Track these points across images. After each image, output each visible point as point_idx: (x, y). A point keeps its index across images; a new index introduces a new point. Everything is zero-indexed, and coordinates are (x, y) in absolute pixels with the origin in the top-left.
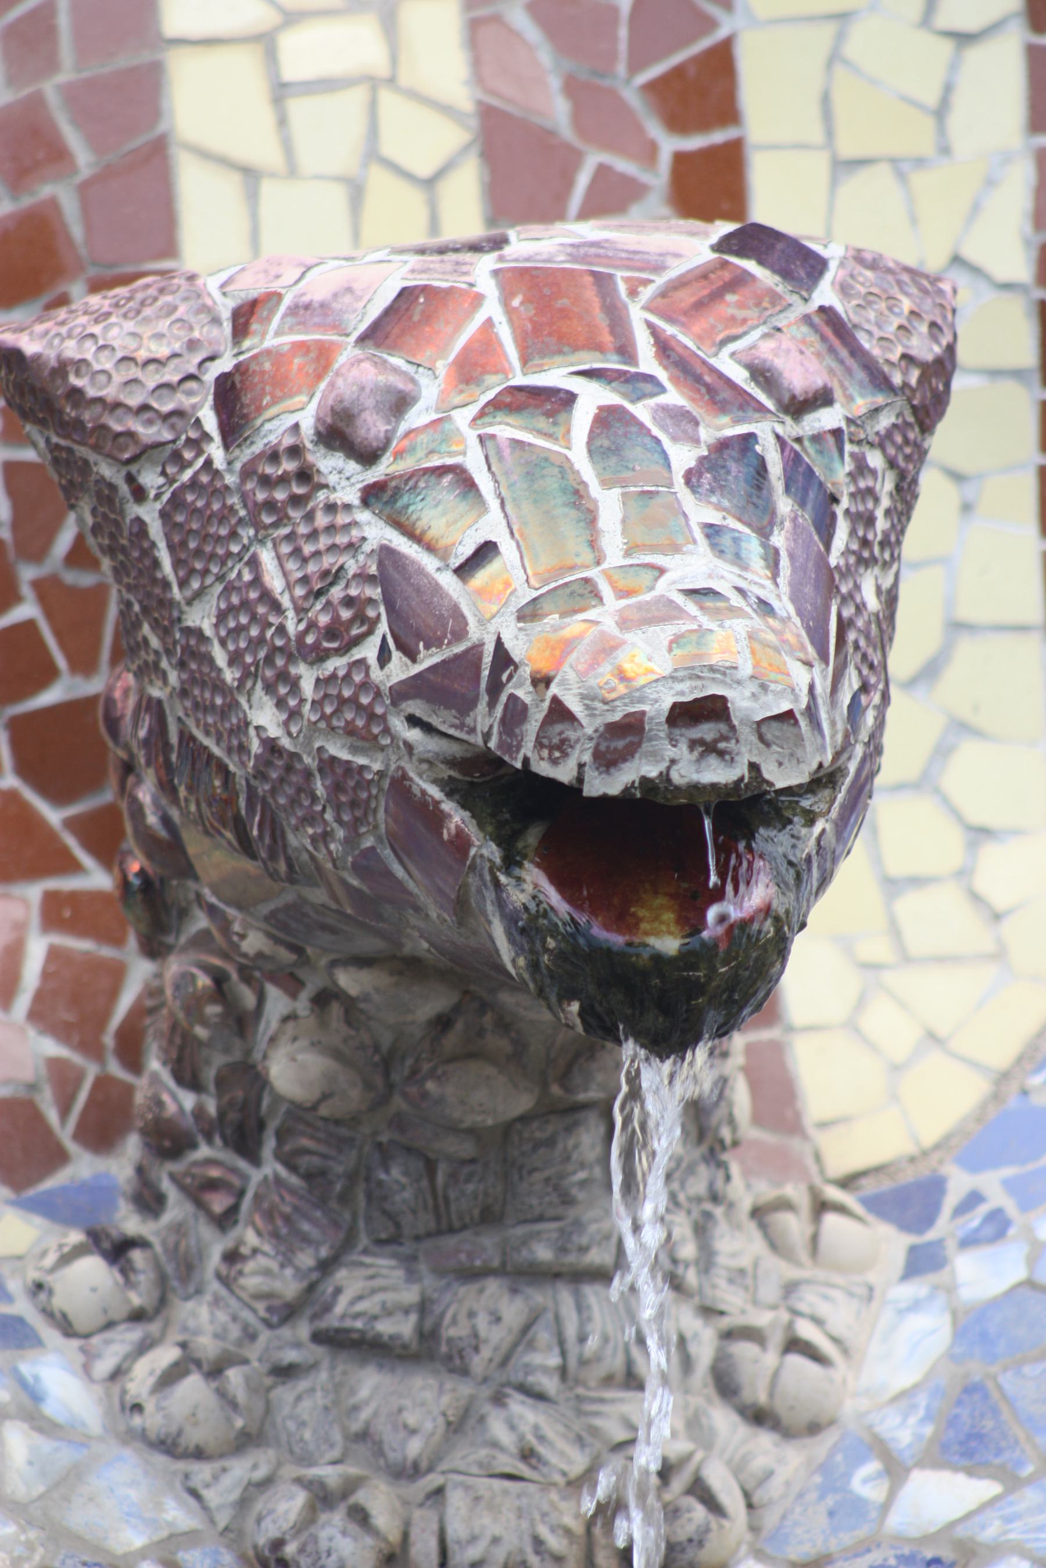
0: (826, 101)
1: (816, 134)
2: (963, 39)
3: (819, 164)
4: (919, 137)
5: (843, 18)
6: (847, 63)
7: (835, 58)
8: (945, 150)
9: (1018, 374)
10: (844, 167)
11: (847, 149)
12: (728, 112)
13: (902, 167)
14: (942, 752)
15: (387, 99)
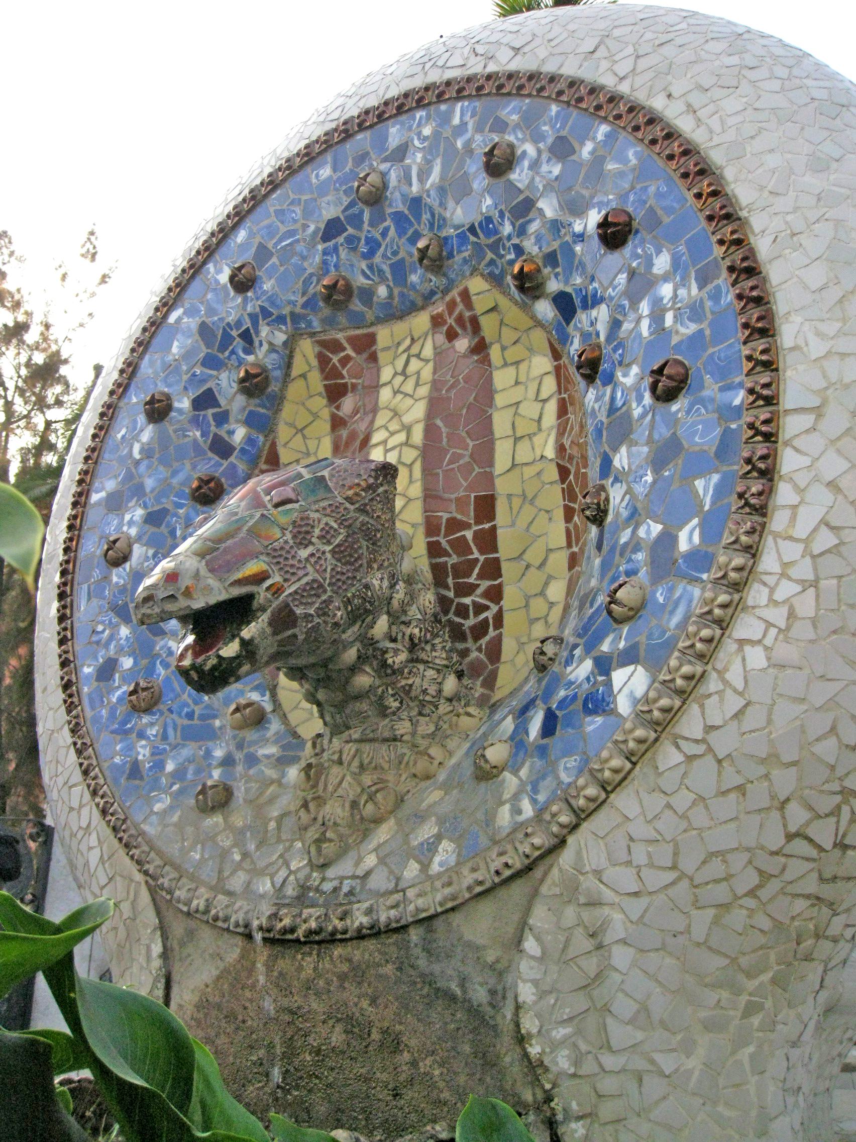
0: (513, 424)
1: (510, 433)
2: (545, 401)
3: (512, 440)
4: (533, 427)
5: (518, 403)
6: (520, 415)
7: (516, 413)
8: (540, 430)
9: (555, 482)
10: (517, 440)
11: (518, 435)
12: (491, 433)
13: (530, 436)
14: (546, 584)
15: (405, 449)
